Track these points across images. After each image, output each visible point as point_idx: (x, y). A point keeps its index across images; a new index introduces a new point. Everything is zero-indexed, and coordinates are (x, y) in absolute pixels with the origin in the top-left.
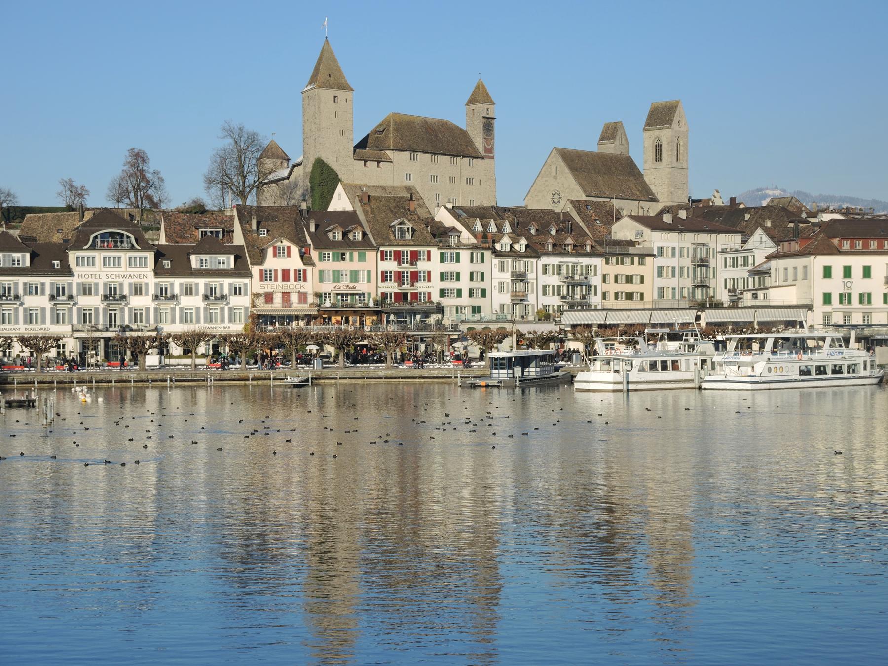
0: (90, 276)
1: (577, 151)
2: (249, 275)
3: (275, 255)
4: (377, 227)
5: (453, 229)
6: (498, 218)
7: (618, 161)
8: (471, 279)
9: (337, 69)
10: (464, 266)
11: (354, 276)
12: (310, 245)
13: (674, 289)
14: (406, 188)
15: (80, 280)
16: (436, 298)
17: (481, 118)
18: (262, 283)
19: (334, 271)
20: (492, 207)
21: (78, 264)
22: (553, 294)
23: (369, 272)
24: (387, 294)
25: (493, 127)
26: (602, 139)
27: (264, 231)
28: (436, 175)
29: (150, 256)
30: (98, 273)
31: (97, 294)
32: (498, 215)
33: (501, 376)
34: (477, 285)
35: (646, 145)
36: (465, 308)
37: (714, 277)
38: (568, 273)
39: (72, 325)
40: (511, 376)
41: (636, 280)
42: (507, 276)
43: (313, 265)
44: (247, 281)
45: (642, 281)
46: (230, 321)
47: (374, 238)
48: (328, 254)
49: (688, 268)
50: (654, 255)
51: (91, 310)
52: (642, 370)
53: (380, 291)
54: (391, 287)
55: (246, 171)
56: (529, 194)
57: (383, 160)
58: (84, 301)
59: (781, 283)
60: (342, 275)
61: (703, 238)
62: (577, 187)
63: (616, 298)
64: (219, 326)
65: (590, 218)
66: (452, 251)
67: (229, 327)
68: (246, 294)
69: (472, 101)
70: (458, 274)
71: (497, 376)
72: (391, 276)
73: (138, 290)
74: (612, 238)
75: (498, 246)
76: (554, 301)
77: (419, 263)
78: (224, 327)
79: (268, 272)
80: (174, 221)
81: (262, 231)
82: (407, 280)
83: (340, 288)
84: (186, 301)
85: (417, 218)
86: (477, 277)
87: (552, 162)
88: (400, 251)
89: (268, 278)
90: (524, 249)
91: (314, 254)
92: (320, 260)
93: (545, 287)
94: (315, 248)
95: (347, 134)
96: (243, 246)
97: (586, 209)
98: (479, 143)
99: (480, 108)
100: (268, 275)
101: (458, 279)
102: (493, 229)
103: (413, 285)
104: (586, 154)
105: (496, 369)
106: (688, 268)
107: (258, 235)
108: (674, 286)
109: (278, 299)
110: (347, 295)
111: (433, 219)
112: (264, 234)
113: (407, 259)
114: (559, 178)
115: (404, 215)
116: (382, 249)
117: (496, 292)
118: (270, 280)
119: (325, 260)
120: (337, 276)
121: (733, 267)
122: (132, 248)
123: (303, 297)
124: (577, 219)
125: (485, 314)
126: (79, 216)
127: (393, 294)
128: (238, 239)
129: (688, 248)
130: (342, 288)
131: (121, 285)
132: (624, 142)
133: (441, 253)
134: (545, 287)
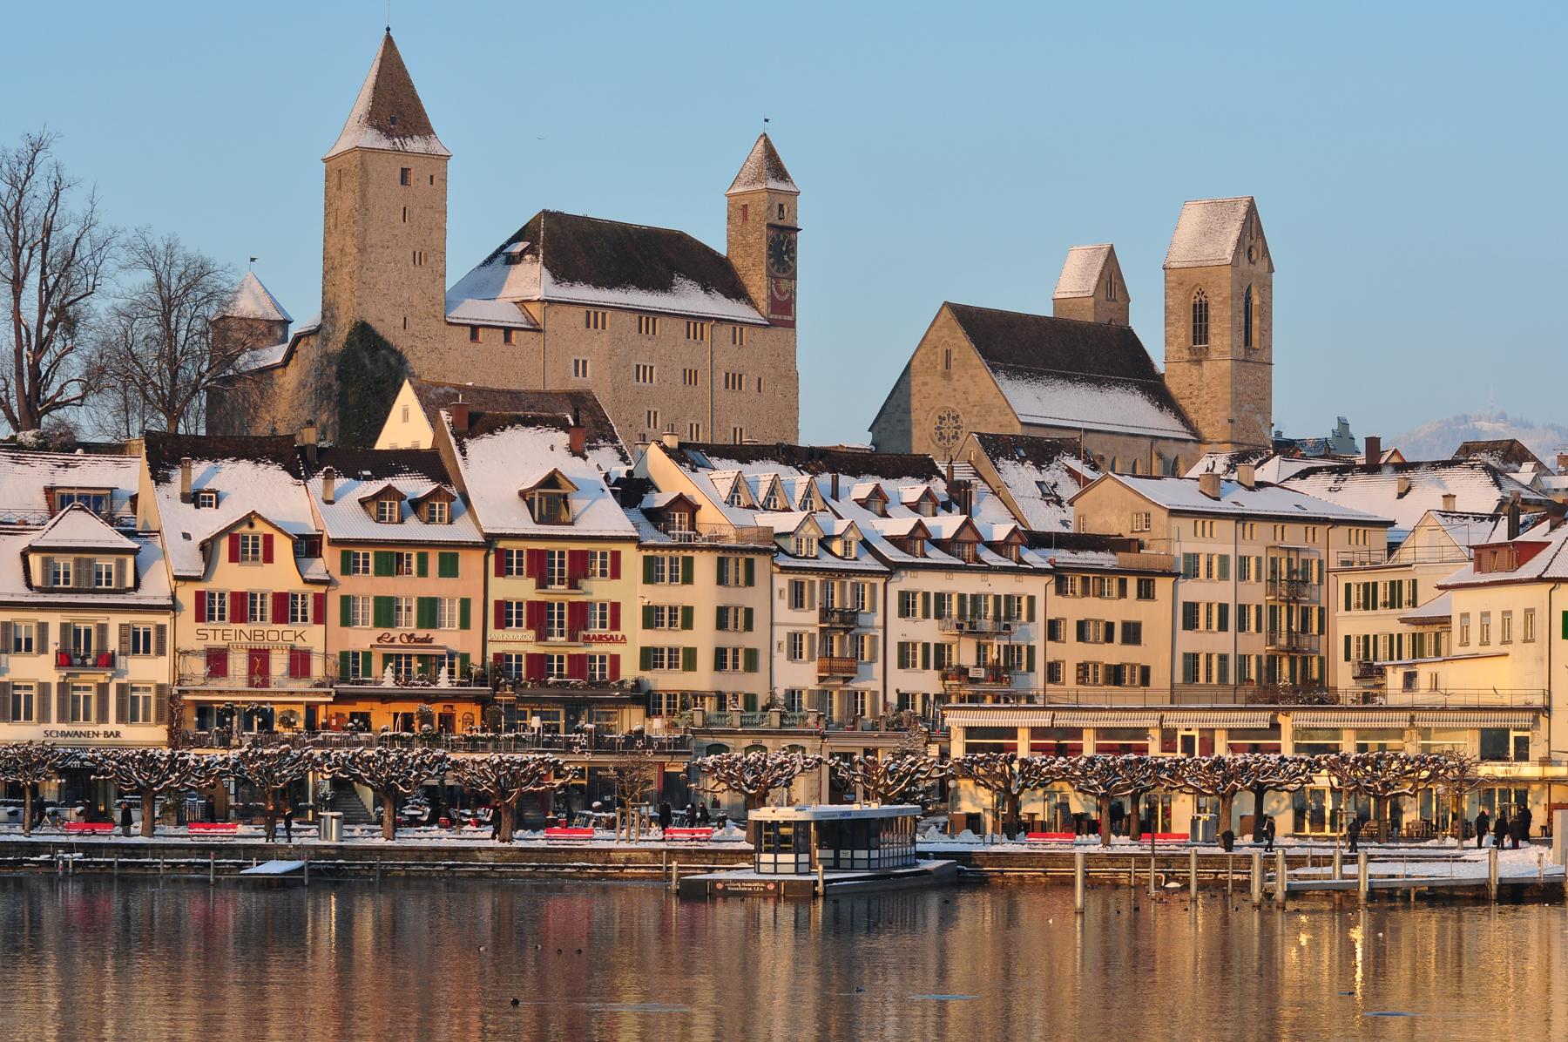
3: (234, 558)
9: (409, 105)
10: (703, 594)
11: (429, 612)
13: (1223, 658)
16: (630, 670)
17: (764, 228)
18: (201, 625)
19: (378, 600)
22: (926, 666)
23: (465, 604)
24: (509, 658)
25: (794, 250)
27: (211, 498)
28: (648, 364)
34: (731, 639)
37: (1321, 631)
38: (962, 615)
42: (808, 620)
46: (121, 718)
48: (366, 556)
49: (1259, 608)
53: (493, 649)
54: (519, 641)
55: (180, 348)
59: (1474, 647)
60: (399, 609)
64: (95, 729)
66: (674, 553)
67: (118, 734)
68: (161, 651)
70: (688, 612)
76: (926, 682)
77: (585, 584)
78: (106, 733)
81: (204, 498)
82: (561, 624)
83: (393, 640)
86: (736, 618)
95: (431, 260)
101: (688, 624)
105: (768, 851)
109: (238, 665)
113: (561, 572)
114: (956, 377)
117: (781, 658)
118: (222, 618)
120: (386, 611)
121: (1366, 608)
123: (300, 663)
129: (1259, 560)
130: (397, 642)
133: (645, 557)
134: (903, 647)
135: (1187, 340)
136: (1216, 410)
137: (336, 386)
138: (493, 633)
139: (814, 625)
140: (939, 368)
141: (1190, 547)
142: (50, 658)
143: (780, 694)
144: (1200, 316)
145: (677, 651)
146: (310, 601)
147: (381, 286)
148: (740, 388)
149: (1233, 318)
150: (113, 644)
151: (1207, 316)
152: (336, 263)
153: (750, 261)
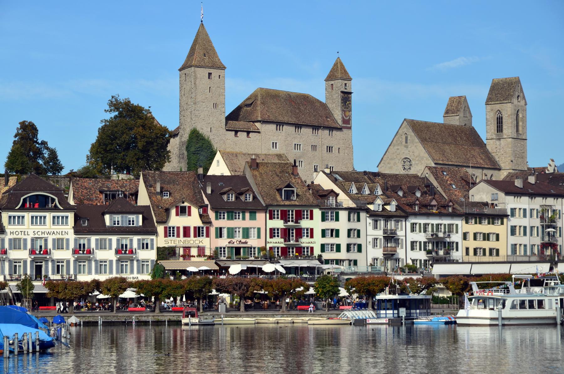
0: (20, 233)
1: (426, 123)
2: (154, 232)
4: (265, 190)
5: (332, 191)
6: (370, 182)
7: (462, 132)
8: (349, 236)
9: (210, 49)
11: (246, 233)
12: (207, 206)
13: (525, 246)
14: (277, 155)
15: (12, 237)
16: (317, 251)
17: (340, 92)
18: (166, 239)
19: (228, 229)
20: (365, 173)
21: (10, 223)
22: (420, 249)
23: (259, 229)
25: (350, 101)
26: (447, 112)
27: (167, 193)
28: (299, 144)
29: (71, 216)
30: (26, 230)
31: (25, 248)
32: (370, 179)
33: (388, 316)
34: (354, 240)
35: (488, 117)
36: (343, 262)
37: (560, 236)
38: (433, 231)
39: (5, 277)
40: (396, 315)
41: (493, 237)
42: (379, 233)
43: (210, 223)
44: (154, 237)
45: (498, 239)
46: (138, 272)
47: (263, 199)
49: (538, 227)
50: (507, 216)
51: (20, 262)
52: (513, 307)
53: (268, 246)
56: (382, 162)
57: (252, 130)
58: (14, 254)
60: (236, 232)
61: (550, 201)
62: (426, 155)
63: (475, 253)
64: (129, 276)
65: (447, 183)
67: (137, 278)
69: (331, 77)
70: (338, 231)
71: (384, 316)
72: (278, 233)
73: (59, 244)
74: (470, 200)
75: (371, 207)
78: (133, 277)
79: (172, 229)
80: (81, 185)
81: (165, 193)
82: (293, 236)
83: (234, 243)
84: (100, 255)
85: (300, 181)
87: (403, 132)
88: (286, 210)
89: (172, 234)
90: (394, 209)
91: (212, 215)
92: (217, 218)
93: (413, 243)
94: (212, 209)
95: (220, 106)
96: (149, 206)
97: (442, 174)
98: (338, 115)
99: (339, 84)
100: (172, 232)
101: (337, 235)
102: (367, 192)
103: (297, 241)
104: (434, 125)
106: (538, 227)
107: (162, 196)
108: (525, 243)
110: (239, 248)
111: (313, 183)
112: (167, 196)
113: (292, 218)
114: (409, 146)
115: (289, 179)
116: (271, 209)
118: (173, 236)
119: (221, 218)
122: (56, 209)
124: (435, 183)
125: (362, 267)
126: (4, 181)
127: (280, 249)
128: (143, 199)
130: (235, 243)
131: (46, 240)
132: (468, 115)
134: (413, 243)
135: (494, 130)
136: (506, 157)
137: (186, 153)
138: (268, 239)
139: (381, 236)
140: (403, 143)
141: (513, 207)
142: (113, 251)
143: (370, 261)
144: (500, 122)
145: (334, 245)
146: (205, 229)
147: (202, 116)
148: (332, 152)
149: (512, 123)
150: (135, 245)
151: (502, 122)
152: (185, 108)
153: (334, 105)
